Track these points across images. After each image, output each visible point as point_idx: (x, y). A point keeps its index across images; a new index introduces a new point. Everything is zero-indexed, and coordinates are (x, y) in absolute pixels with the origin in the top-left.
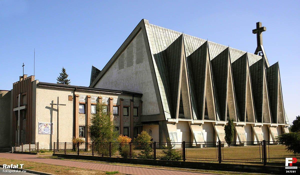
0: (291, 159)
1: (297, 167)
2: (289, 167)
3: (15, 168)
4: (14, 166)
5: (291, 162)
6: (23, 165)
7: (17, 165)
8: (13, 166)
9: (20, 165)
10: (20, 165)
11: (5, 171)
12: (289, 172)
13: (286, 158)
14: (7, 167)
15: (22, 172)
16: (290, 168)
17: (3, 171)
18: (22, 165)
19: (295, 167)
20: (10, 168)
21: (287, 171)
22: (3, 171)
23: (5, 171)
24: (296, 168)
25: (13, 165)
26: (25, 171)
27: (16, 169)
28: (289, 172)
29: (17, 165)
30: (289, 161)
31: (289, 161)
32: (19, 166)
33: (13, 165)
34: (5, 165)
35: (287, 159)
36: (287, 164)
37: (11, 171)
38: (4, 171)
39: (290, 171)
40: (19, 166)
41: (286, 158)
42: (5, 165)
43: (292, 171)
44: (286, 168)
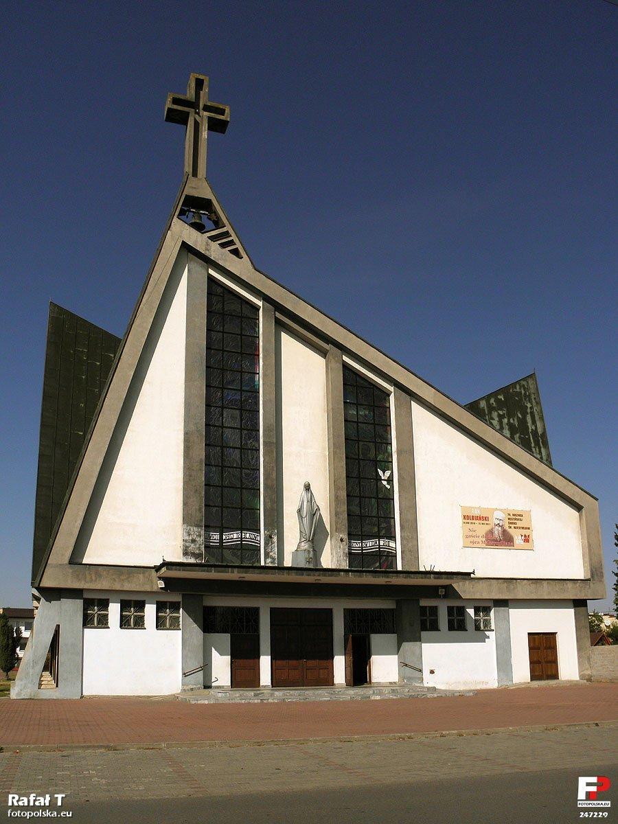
0: (594, 780)
1: (10, 796)
2: (589, 802)
3: (42, 804)
4: (38, 798)
5: (594, 789)
6: (64, 796)
7: (47, 796)
8: (34, 798)
9: (56, 796)
10: (56, 796)
11: (14, 814)
12: (589, 815)
13: (580, 778)
14: (18, 801)
15: (61, 816)
16: (591, 806)
17: (9, 812)
18: (60, 796)
19: (603, 802)
20: (26, 804)
21: (582, 813)
22: (9, 812)
23: (14, 814)
24: (607, 804)
25: (36, 797)
26: (69, 814)
27: (44, 808)
28: (589, 815)
29: (47, 796)
30: (588, 784)
31: (588, 784)
33: (36, 797)
34: (13, 798)
35: (583, 781)
36: (581, 795)
37: (30, 814)
38: (11, 814)
39: (596, 813)
41: (580, 778)
42: (13, 798)
43: (596, 813)
44: (580, 806)
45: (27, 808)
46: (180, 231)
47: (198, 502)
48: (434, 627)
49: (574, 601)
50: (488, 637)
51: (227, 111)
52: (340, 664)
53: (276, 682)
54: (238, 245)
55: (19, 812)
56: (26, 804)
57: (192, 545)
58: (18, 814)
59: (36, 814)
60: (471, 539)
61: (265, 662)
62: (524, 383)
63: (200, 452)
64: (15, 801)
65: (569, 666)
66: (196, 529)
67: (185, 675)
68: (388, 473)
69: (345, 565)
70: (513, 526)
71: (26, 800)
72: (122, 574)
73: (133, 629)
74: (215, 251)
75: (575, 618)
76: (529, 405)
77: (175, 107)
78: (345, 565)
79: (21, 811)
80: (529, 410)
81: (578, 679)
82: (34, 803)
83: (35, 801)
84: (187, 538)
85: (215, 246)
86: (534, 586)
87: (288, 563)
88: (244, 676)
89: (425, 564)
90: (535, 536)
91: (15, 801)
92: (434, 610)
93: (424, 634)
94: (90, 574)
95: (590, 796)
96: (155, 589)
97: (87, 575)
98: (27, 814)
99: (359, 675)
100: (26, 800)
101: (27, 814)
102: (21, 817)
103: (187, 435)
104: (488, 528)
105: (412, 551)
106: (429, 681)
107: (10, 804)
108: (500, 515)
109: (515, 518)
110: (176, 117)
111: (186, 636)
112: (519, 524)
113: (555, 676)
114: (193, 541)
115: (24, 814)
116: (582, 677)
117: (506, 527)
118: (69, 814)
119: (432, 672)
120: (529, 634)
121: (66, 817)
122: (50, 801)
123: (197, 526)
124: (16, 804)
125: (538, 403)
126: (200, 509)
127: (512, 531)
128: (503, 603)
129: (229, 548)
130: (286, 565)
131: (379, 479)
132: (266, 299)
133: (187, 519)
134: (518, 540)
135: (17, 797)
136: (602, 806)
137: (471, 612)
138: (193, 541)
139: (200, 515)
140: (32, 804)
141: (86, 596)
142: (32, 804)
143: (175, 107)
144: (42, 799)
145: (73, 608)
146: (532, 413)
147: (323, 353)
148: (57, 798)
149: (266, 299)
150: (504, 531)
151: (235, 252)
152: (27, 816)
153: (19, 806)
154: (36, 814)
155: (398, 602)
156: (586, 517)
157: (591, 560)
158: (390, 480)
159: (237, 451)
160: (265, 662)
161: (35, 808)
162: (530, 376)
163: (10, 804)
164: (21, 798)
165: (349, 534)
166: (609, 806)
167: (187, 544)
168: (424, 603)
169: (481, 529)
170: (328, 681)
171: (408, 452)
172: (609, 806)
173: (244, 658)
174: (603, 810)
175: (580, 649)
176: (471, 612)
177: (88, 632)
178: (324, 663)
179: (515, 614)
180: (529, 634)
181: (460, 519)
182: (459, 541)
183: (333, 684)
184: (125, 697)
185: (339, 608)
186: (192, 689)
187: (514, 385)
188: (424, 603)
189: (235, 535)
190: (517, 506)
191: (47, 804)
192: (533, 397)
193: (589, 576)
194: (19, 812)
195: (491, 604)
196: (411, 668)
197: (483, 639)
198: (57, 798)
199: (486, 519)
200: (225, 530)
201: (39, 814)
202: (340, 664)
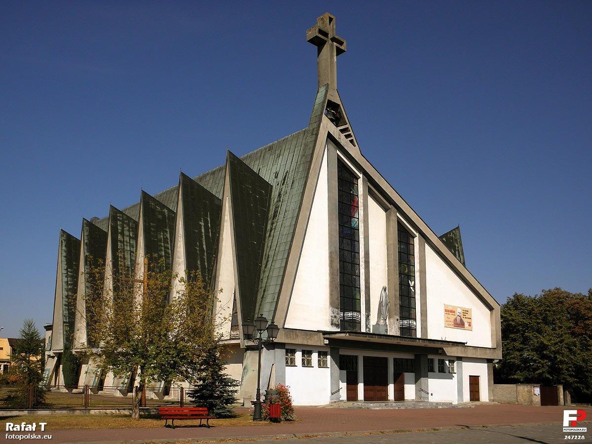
3: (31, 430)
4: (27, 426)
6: (46, 424)
7: (34, 424)
8: (25, 425)
9: (40, 424)
10: (40, 424)
11: (10, 437)
14: (13, 428)
15: (43, 439)
17: (7, 435)
18: (43, 424)
20: (19, 430)
22: (7, 435)
23: (10, 437)
25: (26, 424)
26: (49, 437)
27: (31, 432)
29: (34, 424)
32: (38, 426)
33: (26, 424)
34: (10, 425)
37: (22, 437)
38: (8, 436)
40: (38, 426)
42: (10, 425)
45: (20, 432)
46: (327, 126)
47: (337, 294)
48: (432, 370)
49: (487, 359)
50: (453, 377)
51: (345, 43)
52: (391, 388)
53: (367, 398)
54: (353, 138)
55: (14, 435)
56: (19, 430)
57: (335, 319)
58: (13, 436)
59: (26, 437)
60: (448, 323)
61: (361, 387)
62: (454, 232)
63: (337, 265)
64: (11, 427)
65: (485, 395)
66: (336, 310)
67: (332, 394)
68: (413, 282)
69: (398, 334)
70: (464, 317)
71: (18, 427)
72: (307, 335)
73: (306, 367)
74: (344, 141)
75: (488, 369)
76: (457, 246)
77: (320, 36)
78: (398, 334)
79: (15, 435)
80: (457, 249)
81: (488, 401)
82: (25, 429)
83: (25, 427)
84: (332, 315)
85: (343, 136)
86: (474, 350)
87: (371, 332)
88: (352, 395)
89: (431, 336)
90: (473, 324)
91: (11, 427)
92: (432, 360)
93: (430, 374)
94: (293, 335)
96: (322, 344)
97: (292, 336)
98: (20, 437)
99: (400, 395)
100: (18, 427)
101: (20, 437)
102: (15, 439)
103: (331, 254)
104: (454, 317)
105: (424, 328)
106: (432, 399)
107: (7, 430)
108: (459, 310)
109: (466, 312)
110: (318, 43)
111: (332, 372)
112: (467, 316)
113: (478, 400)
114: (335, 317)
115: (17, 437)
116: (490, 400)
117: (462, 318)
118: (49, 437)
119: (432, 395)
120: (470, 376)
121: (48, 439)
122: (36, 428)
123: (337, 308)
124: (11, 430)
125: (461, 245)
126: (338, 298)
127: (464, 320)
128: (460, 359)
129: (347, 321)
130: (362, 331)
131: (409, 286)
132: (365, 174)
133: (332, 304)
134: (466, 325)
135: (12, 425)
137: (447, 362)
138: (335, 317)
139: (338, 302)
140: (23, 430)
141: (287, 347)
142: (23, 430)
143: (320, 36)
144: (30, 426)
145: (280, 353)
146: (458, 250)
147: (386, 209)
148: (41, 425)
149: (365, 174)
150: (461, 319)
151: (352, 141)
152: (19, 439)
153: (13, 431)
154: (26, 437)
155: (415, 355)
156: (495, 314)
157: (497, 338)
158: (414, 287)
159: (350, 265)
160: (361, 387)
161: (25, 432)
162: (458, 228)
163: (7, 430)
164: (15, 426)
165: (400, 317)
167: (333, 318)
168: (430, 357)
169: (452, 318)
170: (385, 398)
171: (423, 272)
173: (352, 383)
175: (489, 386)
176: (447, 362)
177: (287, 368)
178: (384, 388)
179: (465, 365)
180: (470, 376)
181: (443, 312)
182: (443, 323)
183: (388, 400)
184: (305, 407)
185: (391, 357)
186: (335, 402)
187: (450, 233)
188: (430, 357)
189: (350, 314)
190: (467, 306)
191: (34, 430)
192: (458, 241)
193: (496, 347)
194: (14, 435)
195: (455, 359)
196: (422, 391)
197: (451, 378)
198: (41, 425)
199: (454, 312)
200: (345, 311)
201: (28, 437)
202: (391, 388)
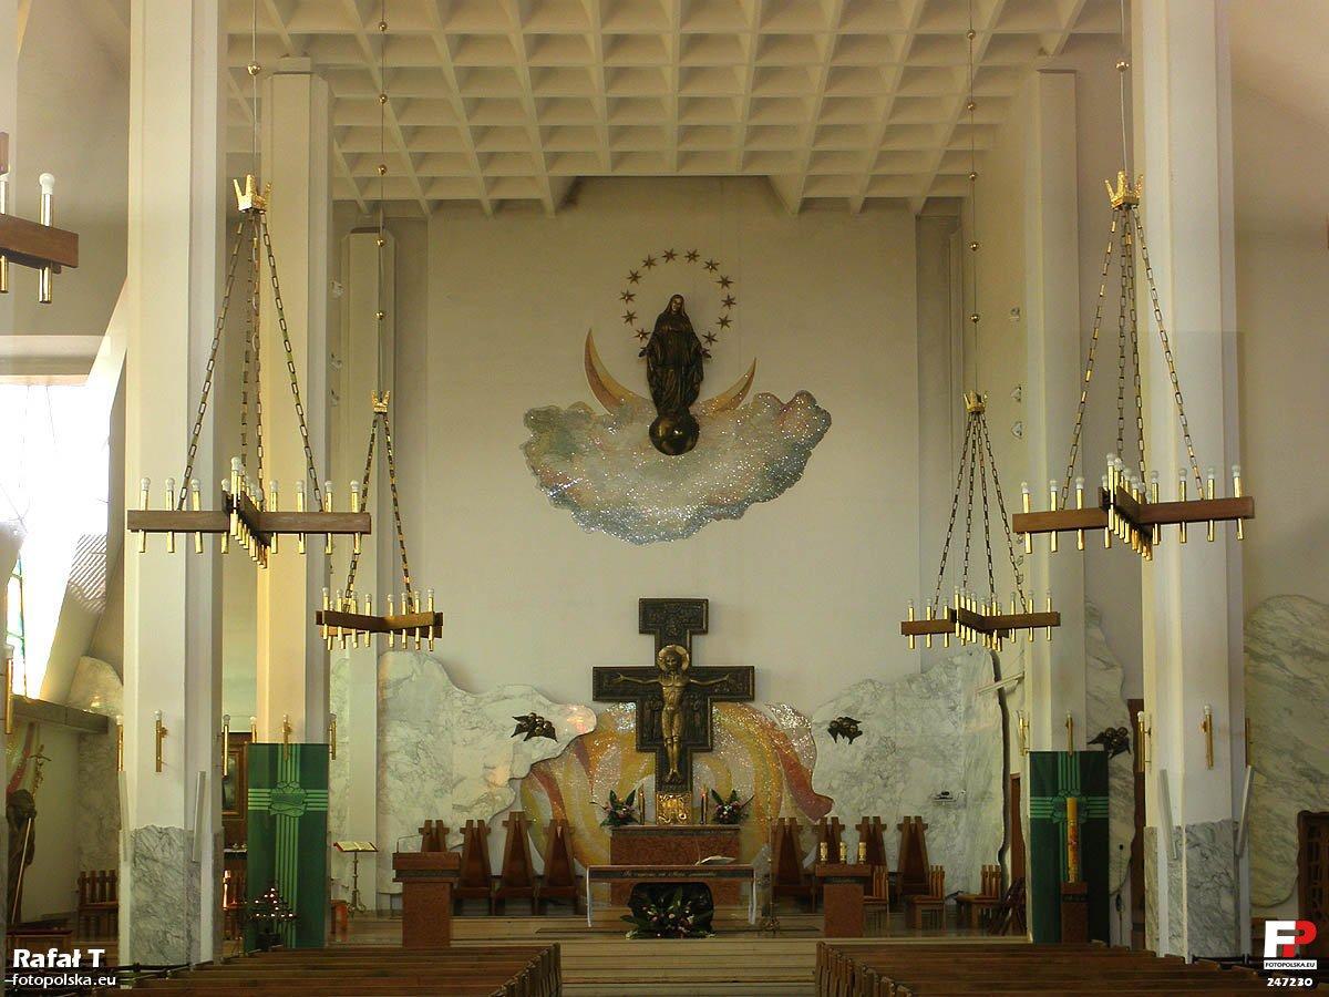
0: (1290, 925)
2: (1282, 962)
3: (68, 965)
4: (61, 956)
5: (1290, 940)
6: (103, 951)
7: (77, 952)
8: (55, 955)
9: (90, 951)
11: (23, 981)
12: (1282, 982)
13: (1267, 922)
14: (29, 961)
16: (1285, 968)
18: (96, 953)
19: (1305, 962)
20: (42, 965)
21: (1271, 980)
23: (23, 981)
24: (1312, 965)
25: (58, 953)
26: (111, 981)
27: (71, 971)
28: (1282, 982)
29: (77, 952)
30: (1281, 933)
31: (1281, 933)
32: (87, 960)
34: (22, 955)
35: (1271, 928)
36: (1270, 950)
37: (49, 981)
39: (1287, 980)
40: (87, 960)
41: (1267, 922)
42: (22, 955)
43: (1294, 980)
44: (1268, 968)
45: (45, 972)
55: (31, 977)
56: (42, 965)
58: (29, 980)
59: (59, 981)
64: (24, 960)
71: (41, 958)
79: (35, 976)
82: (55, 965)
83: (56, 960)
91: (24, 960)
95: (1283, 953)
98: (44, 982)
100: (41, 958)
115: (39, 981)
118: (111, 981)
122: (81, 961)
135: (27, 953)
136: (1302, 968)
140: (51, 965)
148: (92, 955)
154: (59, 981)
161: (57, 971)
163: (16, 965)
164: (34, 956)
166: (1315, 968)
172: (1315, 968)
174: (1304, 974)
191: (76, 965)
194: (31, 977)
198: (92, 955)
201: (64, 981)
